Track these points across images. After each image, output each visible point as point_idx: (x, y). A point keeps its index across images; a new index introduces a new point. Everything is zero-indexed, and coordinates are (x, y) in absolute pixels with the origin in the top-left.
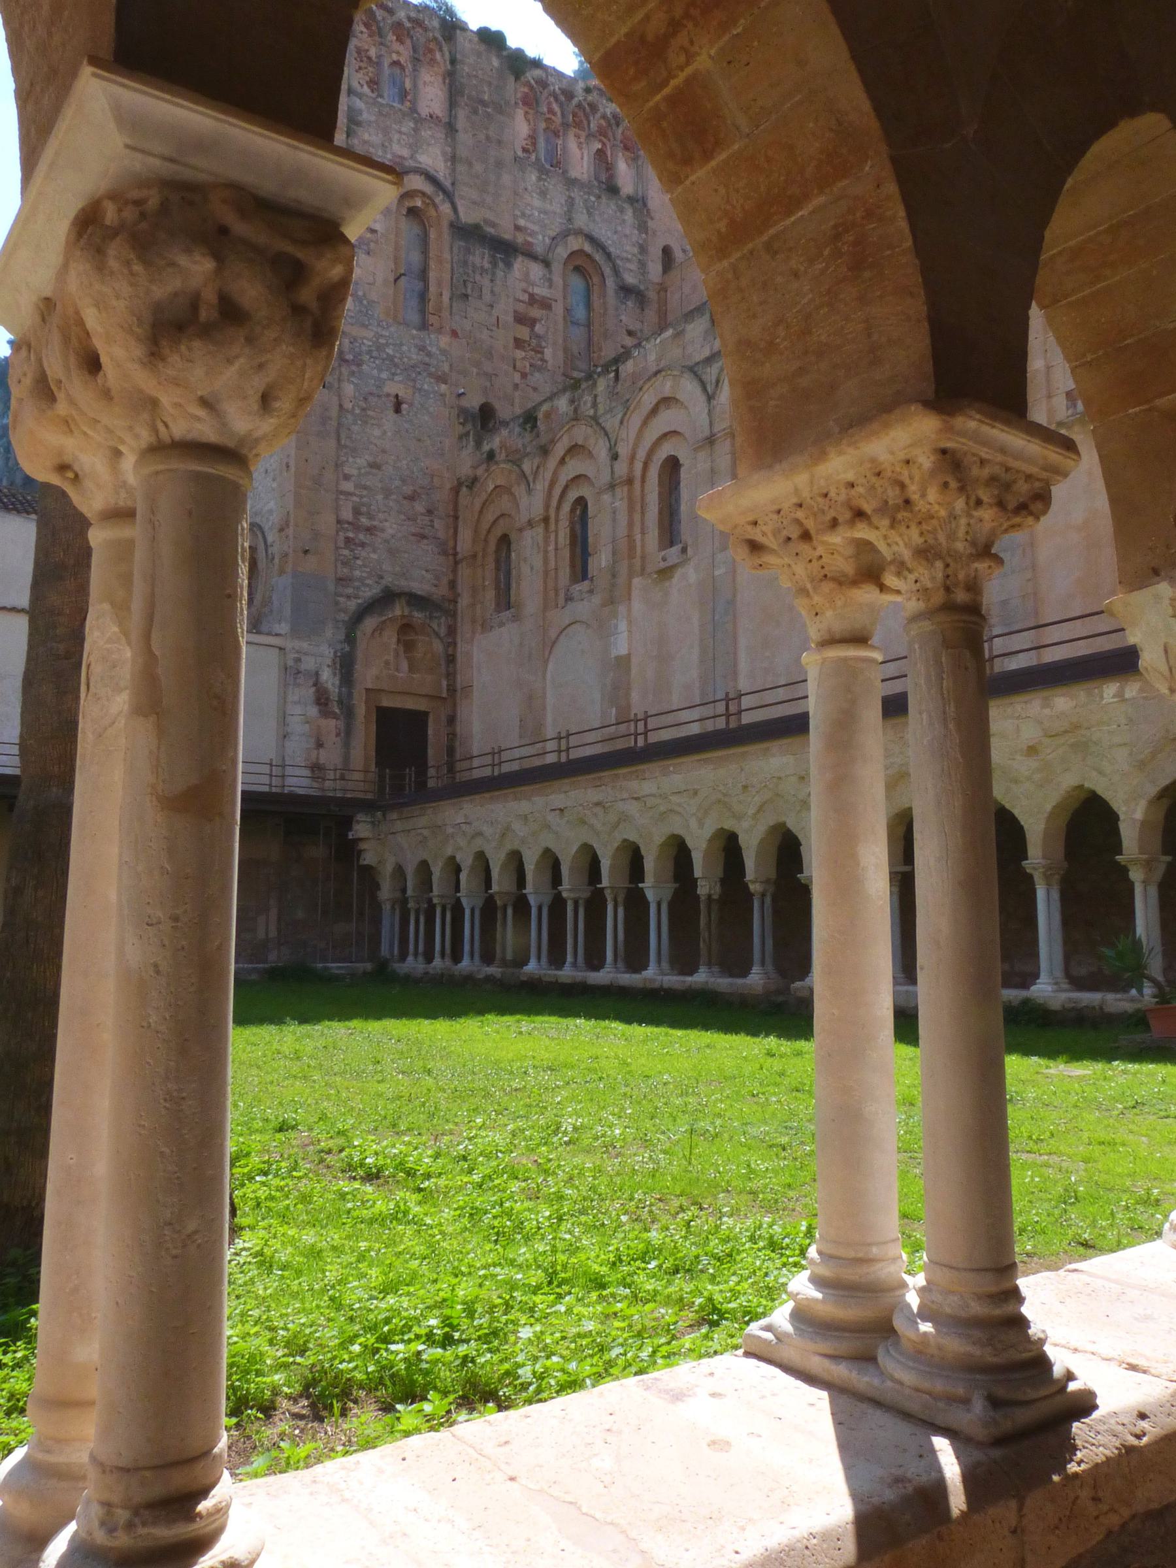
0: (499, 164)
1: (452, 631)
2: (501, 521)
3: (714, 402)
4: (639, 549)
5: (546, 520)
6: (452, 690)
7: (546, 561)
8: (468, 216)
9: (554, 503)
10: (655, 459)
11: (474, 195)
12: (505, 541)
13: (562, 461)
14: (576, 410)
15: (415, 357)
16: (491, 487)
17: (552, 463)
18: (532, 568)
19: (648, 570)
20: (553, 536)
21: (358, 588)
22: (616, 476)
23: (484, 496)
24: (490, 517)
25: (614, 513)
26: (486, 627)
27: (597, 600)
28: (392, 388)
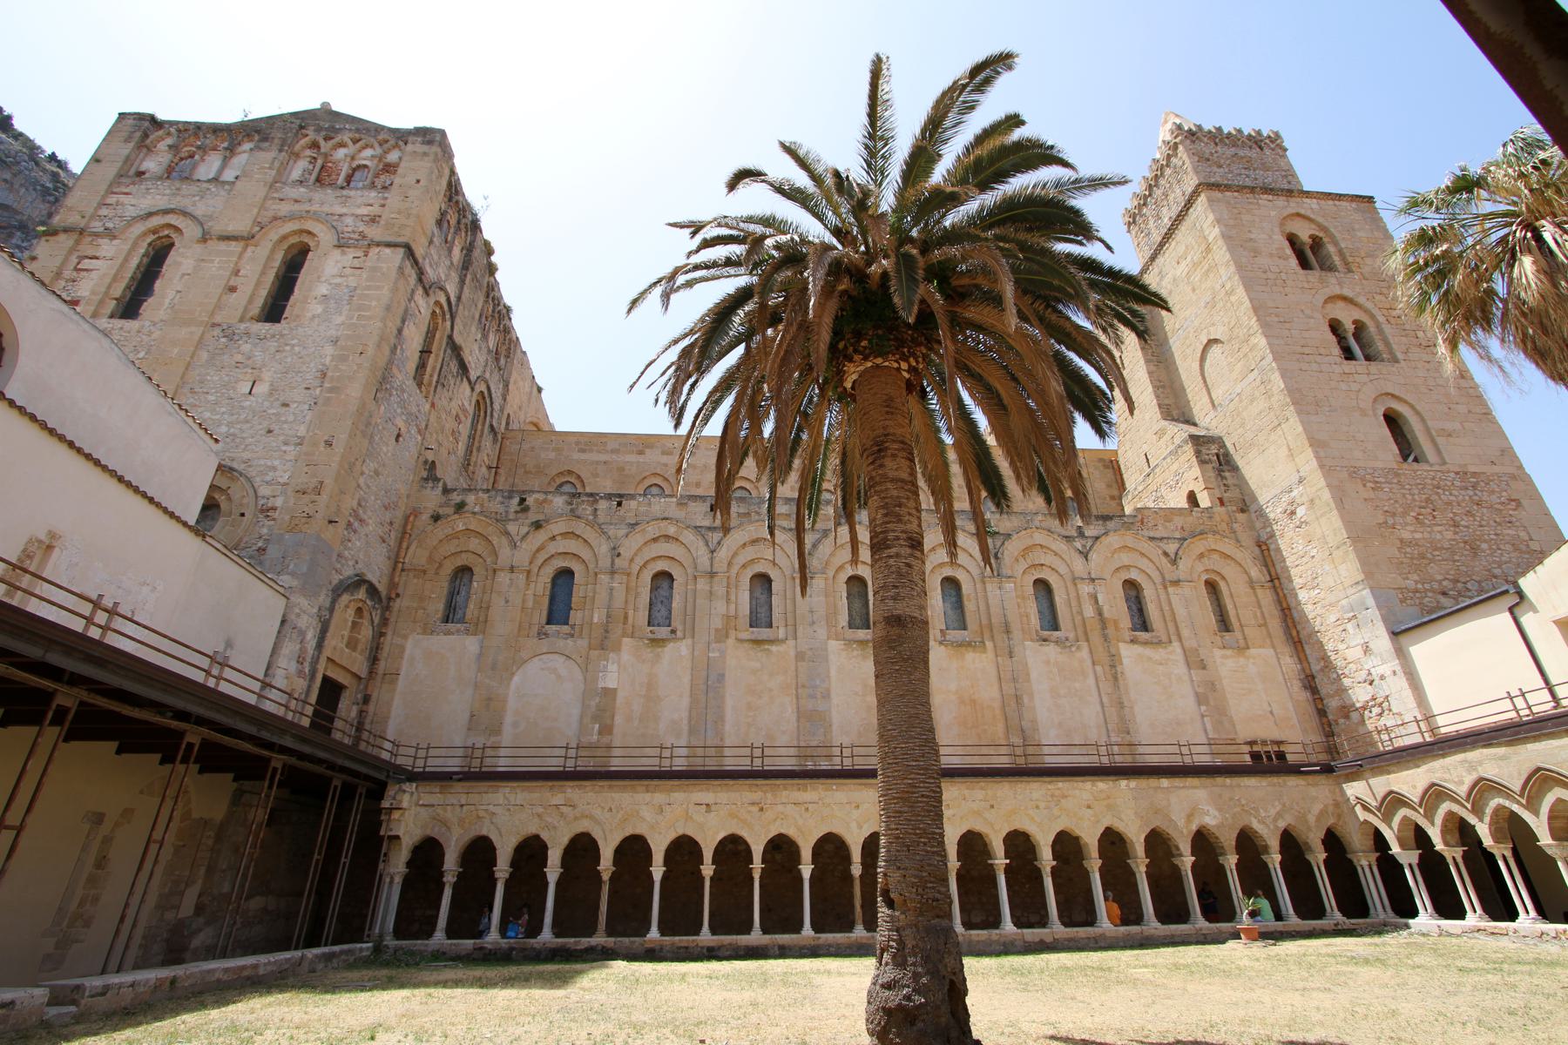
0: (473, 318)
1: (385, 622)
2: (463, 555)
3: (715, 554)
4: (630, 620)
5: (529, 572)
6: (372, 672)
7: (524, 601)
8: (458, 339)
9: (539, 561)
10: (649, 567)
11: (462, 328)
12: (464, 572)
13: (553, 539)
14: (572, 510)
15: (414, 409)
16: (461, 527)
17: (542, 536)
18: (507, 602)
19: (636, 635)
20: (532, 585)
21: (343, 565)
22: (616, 566)
23: (450, 531)
24: (452, 547)
25: (611, 590)
26: (428, 630)
27: (583, 643)
28: (400, 422)
